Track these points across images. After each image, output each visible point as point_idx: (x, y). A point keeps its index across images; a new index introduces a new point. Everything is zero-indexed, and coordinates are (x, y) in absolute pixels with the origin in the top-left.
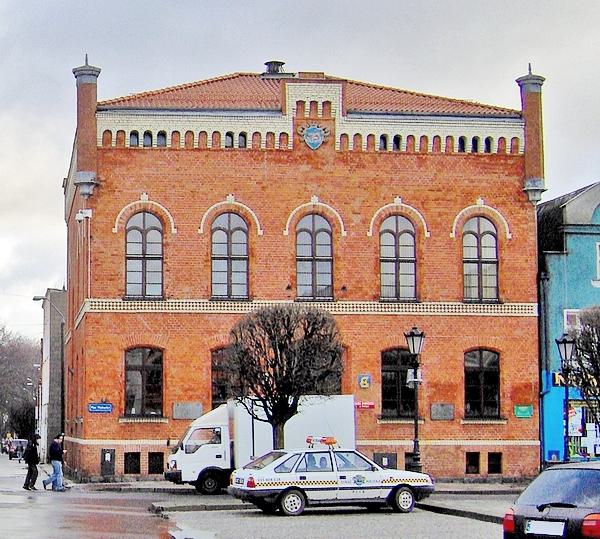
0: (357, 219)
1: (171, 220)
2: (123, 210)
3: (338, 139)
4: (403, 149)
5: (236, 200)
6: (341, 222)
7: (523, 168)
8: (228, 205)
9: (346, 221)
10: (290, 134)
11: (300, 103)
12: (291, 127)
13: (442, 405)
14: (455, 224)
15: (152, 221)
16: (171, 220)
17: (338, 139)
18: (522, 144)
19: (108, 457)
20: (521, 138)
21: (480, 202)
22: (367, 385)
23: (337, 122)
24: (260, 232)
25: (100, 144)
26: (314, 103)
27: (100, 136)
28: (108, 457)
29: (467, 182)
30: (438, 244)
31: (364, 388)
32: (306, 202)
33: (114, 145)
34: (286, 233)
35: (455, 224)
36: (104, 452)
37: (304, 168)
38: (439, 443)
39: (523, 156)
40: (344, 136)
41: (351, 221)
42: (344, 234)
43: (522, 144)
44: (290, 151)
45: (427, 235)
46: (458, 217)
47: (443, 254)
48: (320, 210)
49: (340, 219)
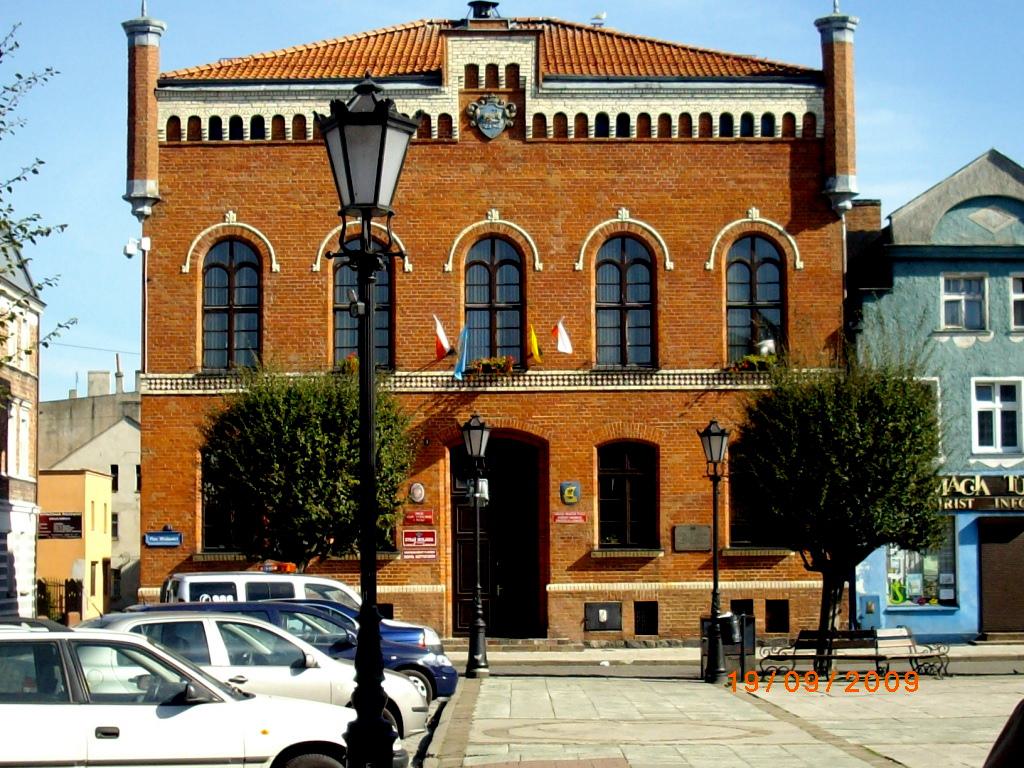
0: (558, 247)
2: (199, 238)
3: (529, 122)
9: (544, 249)
11: (472, 69)
13: (693, 528)
22: (574, 500)
26: (492, 69)
27: (163, 125)
29: (732, 183)
30: (688, 279)
32: (477, 219)
37: (478, 167)
47: (693, 295)
48: (501, 231)
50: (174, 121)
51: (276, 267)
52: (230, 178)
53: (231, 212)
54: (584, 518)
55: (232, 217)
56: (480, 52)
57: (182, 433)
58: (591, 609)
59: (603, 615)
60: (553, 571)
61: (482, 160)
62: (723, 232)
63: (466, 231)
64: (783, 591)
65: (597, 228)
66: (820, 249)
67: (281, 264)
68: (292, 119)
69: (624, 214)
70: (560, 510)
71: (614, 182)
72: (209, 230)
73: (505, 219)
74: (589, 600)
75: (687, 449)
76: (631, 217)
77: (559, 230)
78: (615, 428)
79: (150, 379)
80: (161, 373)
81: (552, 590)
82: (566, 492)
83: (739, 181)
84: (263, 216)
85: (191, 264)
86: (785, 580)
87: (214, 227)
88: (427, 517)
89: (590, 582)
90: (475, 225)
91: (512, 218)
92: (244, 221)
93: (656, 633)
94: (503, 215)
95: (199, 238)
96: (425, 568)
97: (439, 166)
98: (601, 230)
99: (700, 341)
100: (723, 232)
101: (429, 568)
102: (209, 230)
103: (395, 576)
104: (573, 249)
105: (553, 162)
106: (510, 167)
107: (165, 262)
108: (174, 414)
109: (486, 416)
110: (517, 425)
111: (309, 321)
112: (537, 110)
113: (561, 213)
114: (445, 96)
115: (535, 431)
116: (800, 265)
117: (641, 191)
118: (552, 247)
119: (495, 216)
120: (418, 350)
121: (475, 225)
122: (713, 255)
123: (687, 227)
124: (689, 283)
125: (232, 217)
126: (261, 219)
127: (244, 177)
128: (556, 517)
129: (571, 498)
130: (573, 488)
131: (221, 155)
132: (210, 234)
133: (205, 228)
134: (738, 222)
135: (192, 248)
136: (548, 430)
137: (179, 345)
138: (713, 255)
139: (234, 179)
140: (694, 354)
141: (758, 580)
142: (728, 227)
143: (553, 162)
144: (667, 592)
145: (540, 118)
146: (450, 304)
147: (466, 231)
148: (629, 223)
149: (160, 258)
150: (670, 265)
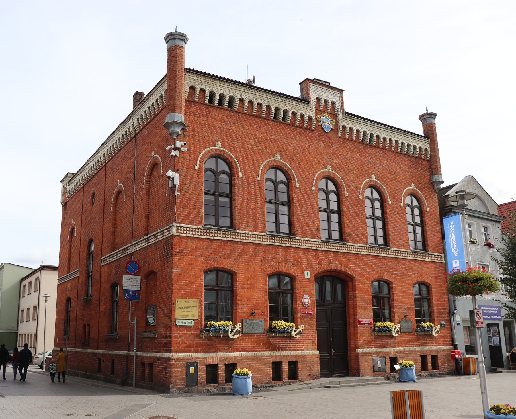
2: (203, 152)
5: (281, 159)
8: (277, 161)
9: (348, 186)
15: (223, 166)
19: (192, 369)
20: (429, 149)
28: (192, 369)
33: (196, 99)
36: (188, 365)
42: (347, 194)
44: (313, 131)
51: (241, 175)
52: (218, 125)
53: (219, 142)
57: (195, 260)
60: (360, 343)
63: (319, 172)
67: (243, 174)
68: (247, 102)
72: (208, 149)
79: (178, 227)
80: (184, 224)
81: (360, 352)
85: (199, 166)
87: (211, 148)
92: (225, 148)
94: (332, 168)
95: (203, 152)
97: (307, 140)
98: (366, 182)
101: (311, 341)
103: (297, 346)
107: (186, 162)
108: (191, 249)
109: (331, 263)
110: (343, 269)
111: (257, 205)
114: (310, 109)
115: (350, 272)
116: (428, 210)
120: (304, 227)
121: (322, 170)
125: (219, 144)
126: (233, 149)
131: (215, 112)
132: (209, 151)
133: (206, 148)
135: (200, 157)
136: (355, 272)
137: (194, 209)
139: (220, 126)
145: (344, 127)
147: (319, 172)
148: (375, 181)
150: (390, 202)
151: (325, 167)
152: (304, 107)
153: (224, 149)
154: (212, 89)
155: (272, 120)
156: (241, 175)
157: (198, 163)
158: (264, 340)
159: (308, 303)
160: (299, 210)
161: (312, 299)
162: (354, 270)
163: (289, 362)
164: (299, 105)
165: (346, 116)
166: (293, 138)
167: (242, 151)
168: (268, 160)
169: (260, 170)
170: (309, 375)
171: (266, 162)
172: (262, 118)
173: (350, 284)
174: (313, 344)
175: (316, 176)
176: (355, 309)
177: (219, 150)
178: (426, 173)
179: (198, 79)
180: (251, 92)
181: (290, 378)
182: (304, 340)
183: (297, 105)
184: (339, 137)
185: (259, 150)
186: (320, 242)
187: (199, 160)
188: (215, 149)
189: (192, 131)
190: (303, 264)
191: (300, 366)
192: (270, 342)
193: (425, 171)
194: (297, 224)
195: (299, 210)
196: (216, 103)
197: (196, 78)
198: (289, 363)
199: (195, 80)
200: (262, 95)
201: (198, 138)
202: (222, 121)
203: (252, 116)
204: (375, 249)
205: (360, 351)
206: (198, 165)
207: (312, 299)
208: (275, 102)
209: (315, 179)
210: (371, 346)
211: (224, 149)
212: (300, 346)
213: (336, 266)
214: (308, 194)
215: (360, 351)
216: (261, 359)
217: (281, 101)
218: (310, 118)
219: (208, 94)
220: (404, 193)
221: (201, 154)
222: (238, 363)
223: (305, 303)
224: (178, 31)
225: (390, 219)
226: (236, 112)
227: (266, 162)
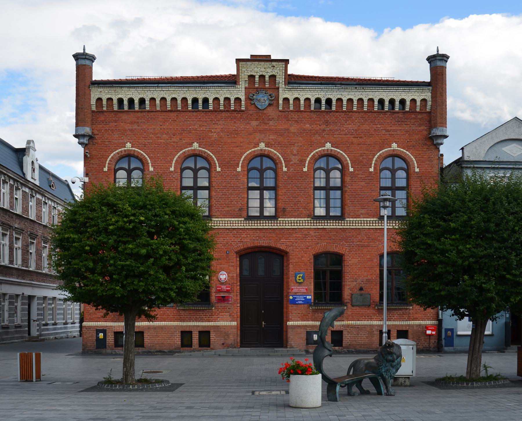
0: (295, 160)
1: (149, 161)
2: (112, 155)
3: (281, 102)
4: (334, 108)
5: (199, 147)
6: (283, 162)
7: (430, 121)
8: (195, 150)
10: (243, 98)
11: (252, 77)
12: (243, 94)
14: (374, 162)
16: (149, 161)
17: (281, 102)
18: (429, 103)
21: (394, 146)
22: (302, 281)
23: (280, 90)
24: (219, 169)
25: (94, 108)
26: (262, 77)
27: (93, 102)
30: (360, 176)
31: (300, 283)
32: (255, 147)
34: (239, 169)
35: (374, 162)
37: (254, 123)
38: (358, 323)
39: (430, 113)
40: (286, 100)
41: (290, 160)
42: (285, 169)
43: (429, 103)
44: (243, 111)
45: (351, 169)
46: (376, 156)
47: (363, 184)
48: (266, 153)
49: (282, 159)
50: (99, 100)
51: (151, 169)
52: (128, 127)
53: (128, 143)
54: (306, 289)
55: (129, 145)
56: (256, 69)
58: (309, 335)
59: (315, 337)
61: (257, 120)
62: (378, 154)
63: (248, 152)
64: (406, 325)
65: (315, 152)
66: (428, 162)
68: (159, 99)
69: (328, 146)
70: (294, 286)
71: (324, 130)
72: (117, 151)
73: (268, 147)
74: (308, 329)
75: (359, 257)
76: (332, 147)
77: (295, 152)
78: (322, 246)
82: (298, 277)
83: (388, 131)
84: (145, 145)
85: (108, 167)
86: (407, 320)
88: (227, 289)
89: (309, 321)
90: (253, 150)
91: (272, 146)
93: (342, 346)
96: (226, 313)
98: (317, 153)
99: (366, 205)
100: (378, 154)
101: (228, 313)
102: (117, 151)
104: (302, 162)
105: (293, 121)
106: (271, 123)
107: (95, 166)
109: (257, 240)
110: (273, 245)
112: (285, 96)
113: (296, 145)
114: (239, 90)
115: (283, 247)
117: (337, 134)
118: (292, 160)
119: (262, 146)
120: (223, 208)
121: (253, 150)
122: (373, 165)
123: (361, 152)
124: (362, 178)
125: (129, 145)
127: (135, 127)
128: (292, 289)
129: (300, 280)
130: (301, 275)
131: (124, 116)
132: (118, 153)
134: (386, 150)
135: (109, 159)
136: (290, 247)
138: (373, 165)
139: (131, 128)
140: (363, 211)
141: (393, 320)
142: (381, 152)
143: (293, 121)
144: (348, 326)
146: (240, 187)
147: (248, 152)
149: (93, 164)
151: (257, 145)
152: (230, 90)
153: (133, 149)
154: (120, 96)
155: (190, 111)
156: (151, 169)
157: (107, 165)
158: (173, 312)
159: (225, 279)
160: (219, 192)
161: (231, 275)
162: (289, 245)
163: (199, 332)
164: (223, 89)
165: (289, 87)
166: (218, 124)
167: (154, 146)
168: (184, 151)
169: (174, 162)
170: (223, 344)
171: (181, 152)
172: (179, 111)
173: (285, 258)
174: (230, 316)
175: (243, 157)
176: (288, 283)
177: (128, 150)
178: (423, 127)
179: (104, 90)
180: (163, 89)
181: (201, 345)
182: (219, 312)
183: (221, 89)
184: (280, 111)
185: (174, 142)
186: (244, 221)
187: (107, 162)
188: (125, 150)
189: (101, 138)
190: (220, 243)
191: (213, 336)
192: (180, 314)
193: (420, 125)
194: (215, 207)
195: (219, 192)
196: (126, 108)
197: (102, 90)
198: (200, 333)
199: (101, 92)
200: (176, 90)
201: (107, 143)
202: (132, 123)
203: (166, 111)
204: (320, 222)
205: (290, 323)
206: (107, 167)
207: (231, 275)
208: (193, 93)
209: (242, 159)
210: (306, 319)
211: (133, 149)
212: (214, 317)
213: (263, 242)
214: (232, 176)
215: (290, 323)
216: (169, 328)
217: (201, 90)
218: (238, 100)
219: (115, 102)
220: (376, 156)
221: (110, 157)
222: (144, 331)
223: (220, 279)
224: (87, 51)
225: (348, 188)
226: (148, 111)
227: (181, 152)
